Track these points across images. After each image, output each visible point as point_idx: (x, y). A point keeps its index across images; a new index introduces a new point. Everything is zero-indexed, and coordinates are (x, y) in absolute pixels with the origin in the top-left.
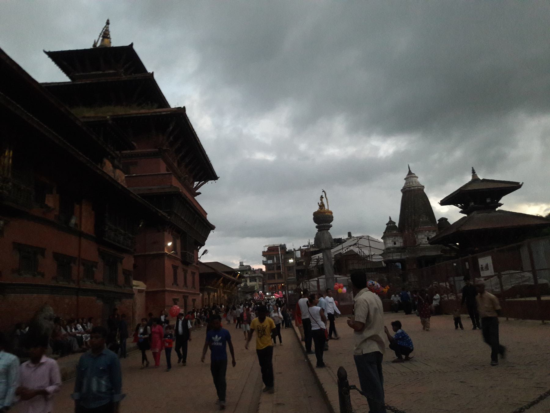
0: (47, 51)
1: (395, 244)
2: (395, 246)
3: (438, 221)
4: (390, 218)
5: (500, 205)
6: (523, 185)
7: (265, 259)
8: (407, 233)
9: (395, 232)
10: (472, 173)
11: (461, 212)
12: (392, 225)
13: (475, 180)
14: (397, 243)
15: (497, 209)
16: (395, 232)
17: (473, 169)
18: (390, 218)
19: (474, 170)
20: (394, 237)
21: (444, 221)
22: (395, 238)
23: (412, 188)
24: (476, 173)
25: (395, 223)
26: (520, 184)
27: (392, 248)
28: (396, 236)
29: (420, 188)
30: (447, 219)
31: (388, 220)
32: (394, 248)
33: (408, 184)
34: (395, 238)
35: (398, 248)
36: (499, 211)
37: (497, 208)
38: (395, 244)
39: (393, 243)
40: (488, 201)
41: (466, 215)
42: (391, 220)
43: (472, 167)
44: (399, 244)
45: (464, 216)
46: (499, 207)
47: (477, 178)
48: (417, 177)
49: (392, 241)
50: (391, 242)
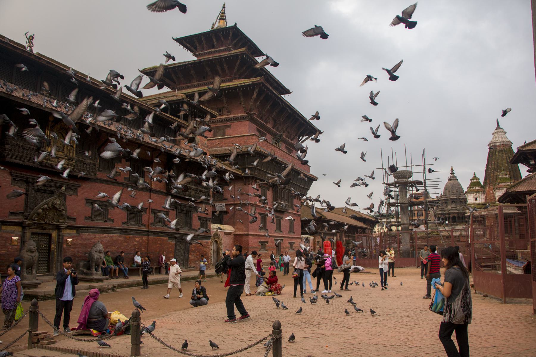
0: (175, 38)
1: (476, 199)
2: (477, 202)
4: (475, 174)
8: (487, 189)
9: (477, 188)
12: (475, 180)
14: (478, 199)
16: (477, 188)
18: (475, 174)
20: (475, 193)
23: (498, 144)
28: (477, 192)
29: (506, 143)
31: (473, 176)
32: (474, 204)
33: (494, 139)
35: (479, 204)
38: (476, 199)
39: (474, 199)
44: (481, 200)
48: (506, 133)
50: (472, 198)
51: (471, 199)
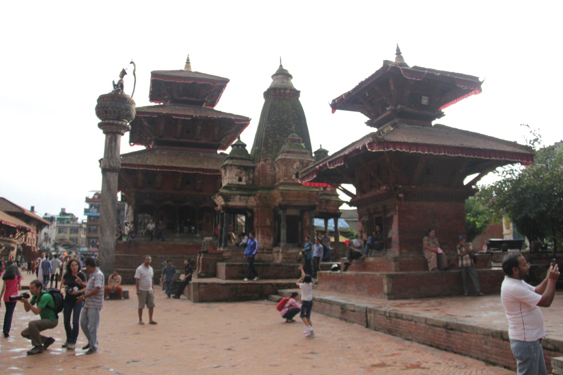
1: (240, 180)
2: (241, 183)
3: (315, 153)
5: (441, 115)
6: (484, 82)
7: (87, 206)
10: (396, 54)
11: (369, 124)
14: (244, 179)
15: (434, 123)
17: (398, 47)
19: (400, 48)
21: (323, 153)
22: (241, 173)
24: (401, 55)
25: (245, 145)
26: (481, 80)
27: (232, 186)
30: (328, 152)
34: (241, 173)
36: (437, 126)
37: (435, 119)
38: (240, 180)
39: (237, 178)
40: (425, 101)
41: (375, 130)
42: (240, 140)
43: (397, 45)
45: (372, 132)
46: (437, 119)
47: (404, 62)
49: (236, 175)
50: (234, 176)
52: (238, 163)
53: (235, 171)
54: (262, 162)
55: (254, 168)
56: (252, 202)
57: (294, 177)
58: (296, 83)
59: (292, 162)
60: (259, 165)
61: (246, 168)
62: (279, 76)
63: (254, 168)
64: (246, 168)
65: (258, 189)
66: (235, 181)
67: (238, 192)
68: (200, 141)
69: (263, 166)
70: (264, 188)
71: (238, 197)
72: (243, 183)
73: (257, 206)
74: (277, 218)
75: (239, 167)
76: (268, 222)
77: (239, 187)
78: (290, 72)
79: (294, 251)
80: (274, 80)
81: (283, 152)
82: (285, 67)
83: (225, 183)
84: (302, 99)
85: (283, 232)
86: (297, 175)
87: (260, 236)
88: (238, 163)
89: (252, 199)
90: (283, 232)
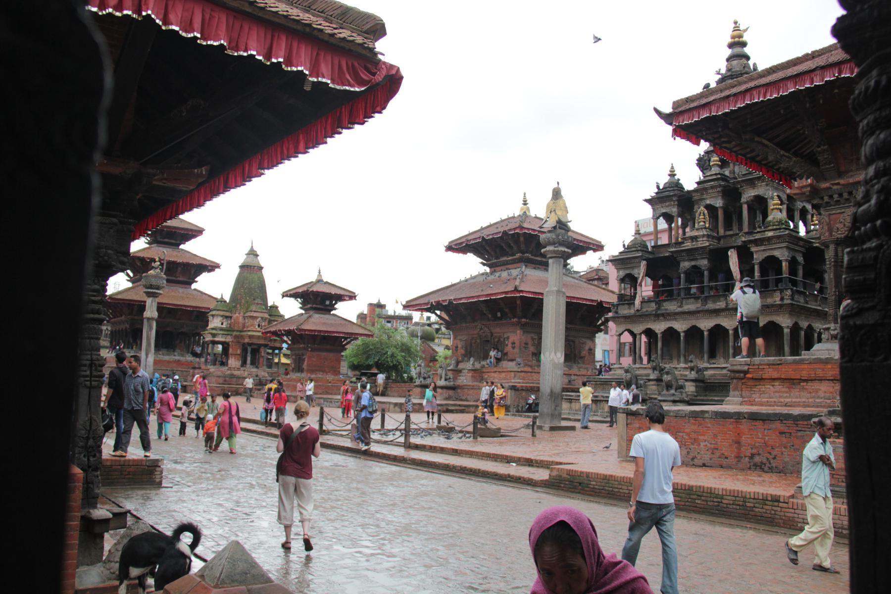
1: (222, 324)
5: (335, 309)
11: (301, 308)
13: (320, 281)
14: (225, 324)
15: (332, 313)
36: (334, 315)
38: (222, 324)
51: (215, 323)
52: (221, 313)
53: (220, 319)
54: (237, 315)
55: (231, 317)
56: (229, 339)
57: (257, 327)
58: (262, 261)
59: (256, 318)
60: (235, 316)
61: (227, 317)
62: (252, 256)
63: (231, 317)
64: (227, 317)
65: (234, 331)
66: (219, 325)
67: (221, 332)
68: (178, 279)
69: (237, 317)
70: (237, 331)
71: (220, 336)
72: (224, 326)
73: (232, 342)
74: (245, 350)
75: (222, 316)
76: (239, 352)
77: (221, 329)
78: (258, 253)
79: (254, 370)
80: (247, 258)
81: (251, 311)
82: (255, 249)
83: (211, 326)
84: (264, 271)
85: (249, 359)
86: (259, 326)
87: (233, 360)
88: (221, 313)
89: (229, 337)
90: (249, 359)
